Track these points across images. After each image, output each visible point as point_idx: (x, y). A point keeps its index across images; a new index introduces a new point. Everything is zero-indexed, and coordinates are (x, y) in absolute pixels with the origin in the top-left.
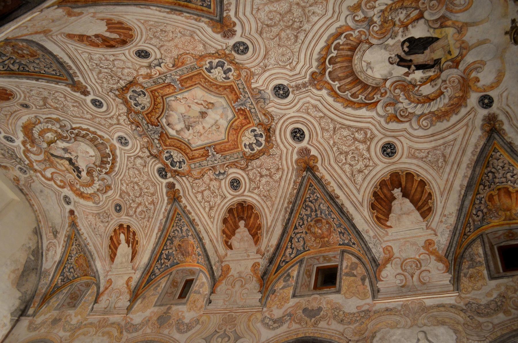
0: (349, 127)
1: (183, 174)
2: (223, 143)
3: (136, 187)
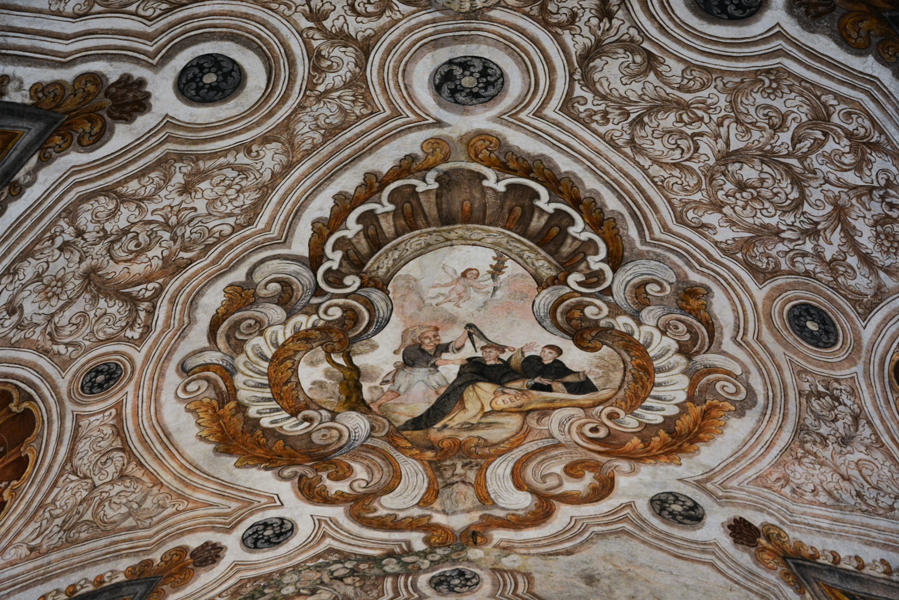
3: (748, 173)
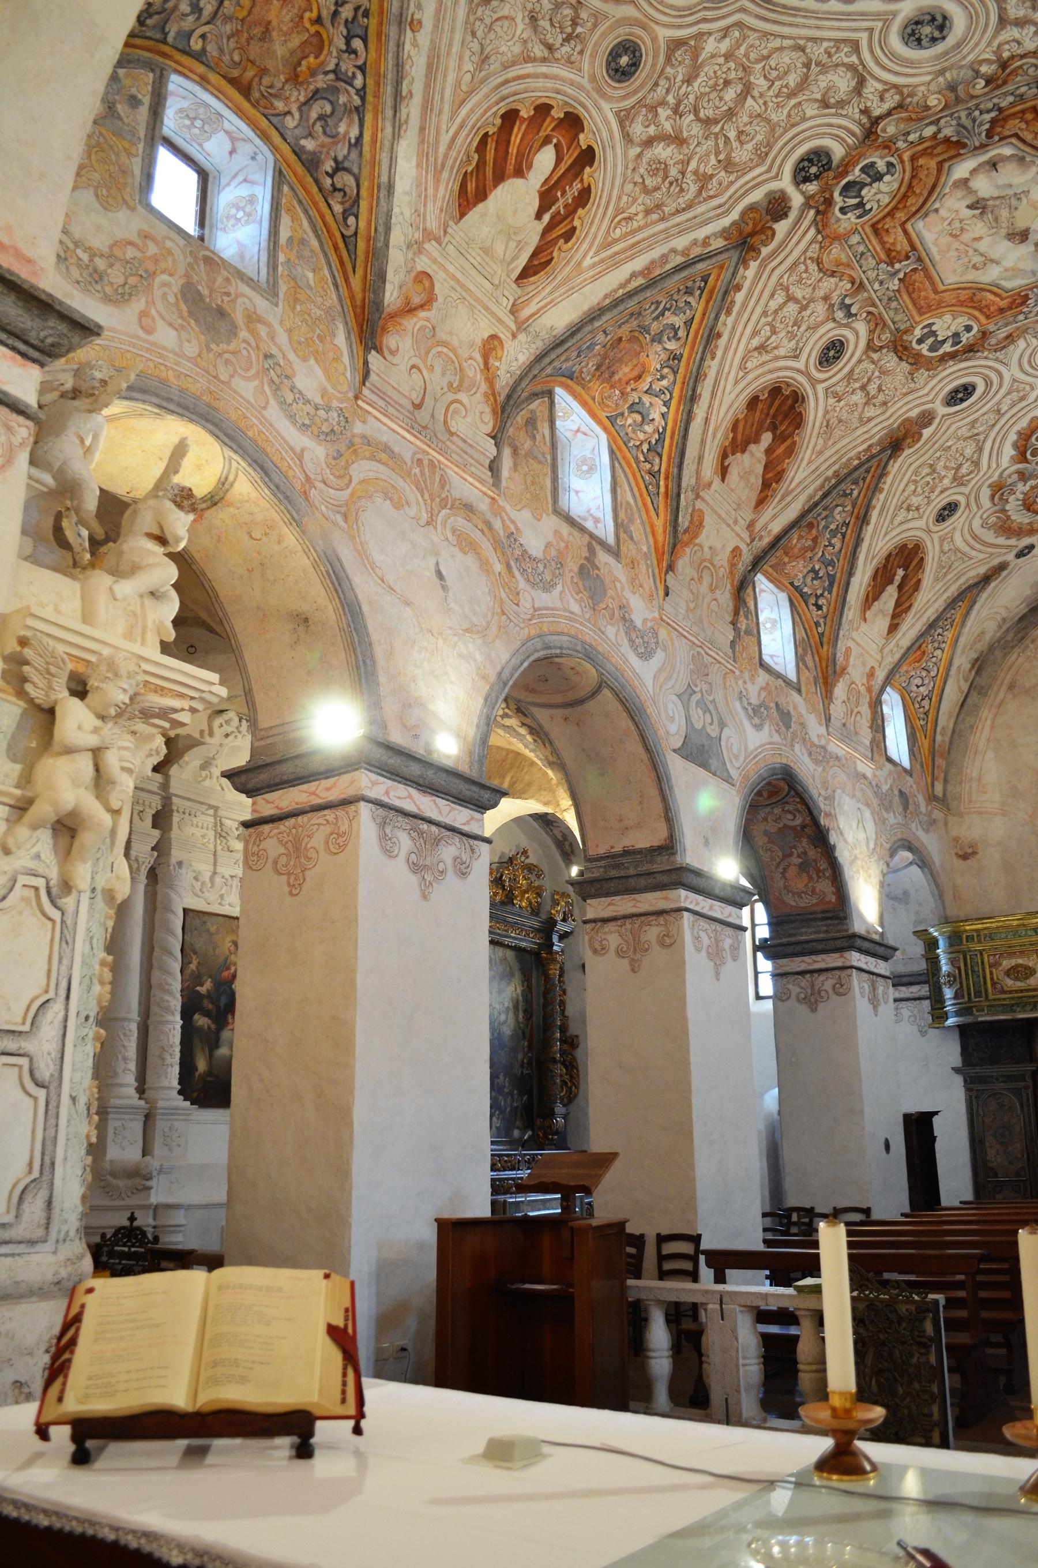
0: (980, 449)
1: (825, 226)
2: (933, 284)
3: (730, 94)
